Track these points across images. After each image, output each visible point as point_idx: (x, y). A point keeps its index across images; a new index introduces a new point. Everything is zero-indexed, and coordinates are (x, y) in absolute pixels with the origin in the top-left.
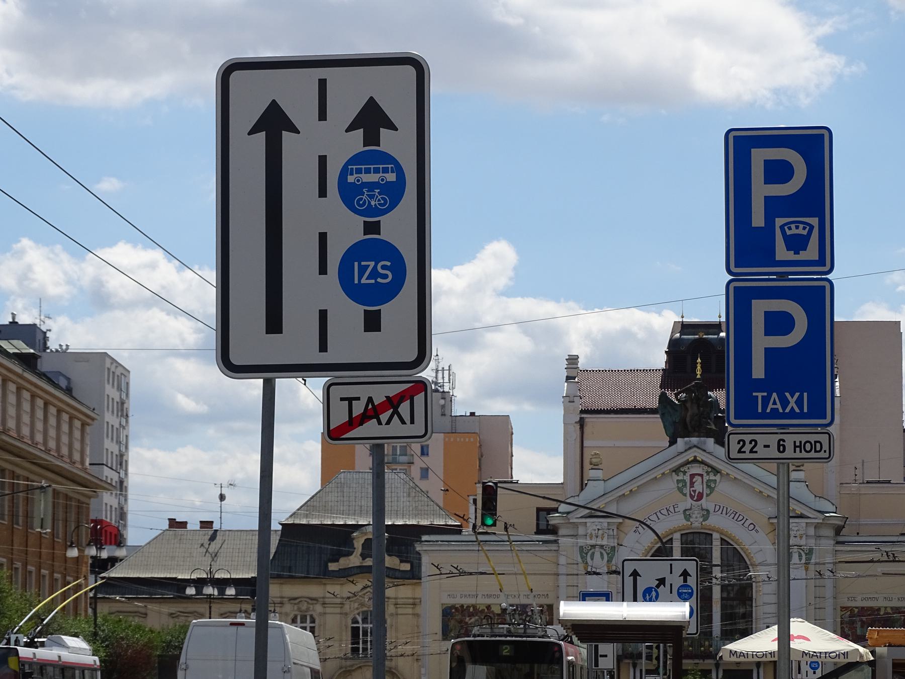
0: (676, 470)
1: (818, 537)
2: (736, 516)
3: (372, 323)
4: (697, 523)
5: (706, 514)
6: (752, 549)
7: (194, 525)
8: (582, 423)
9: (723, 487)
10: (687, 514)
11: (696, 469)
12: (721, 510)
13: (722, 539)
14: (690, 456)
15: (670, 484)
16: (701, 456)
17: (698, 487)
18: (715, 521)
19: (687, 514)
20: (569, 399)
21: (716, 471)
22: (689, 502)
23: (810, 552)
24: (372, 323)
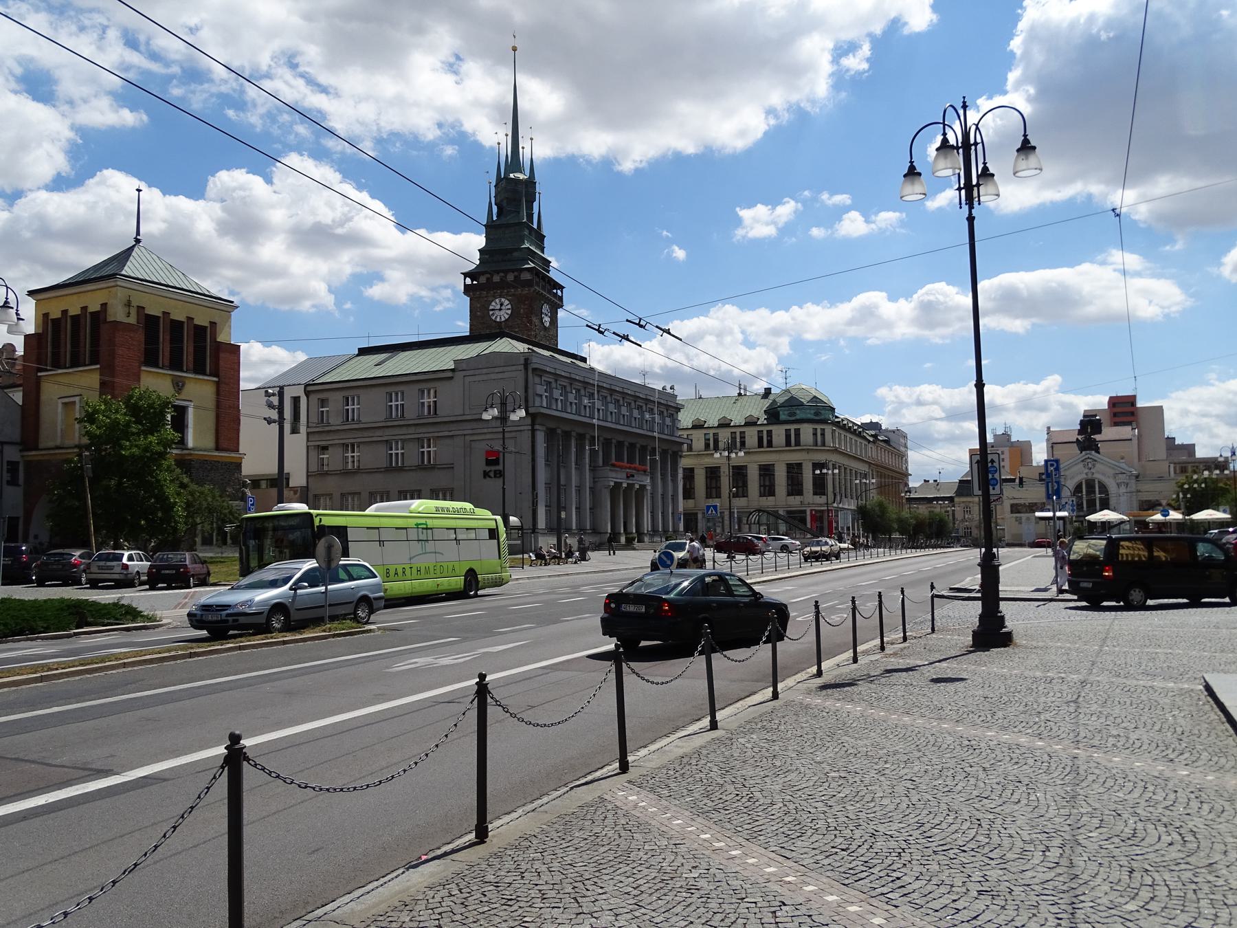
0: (1083, 461)
1: (1130, 479)
2: (1103, 474)
3: (994, 489)
4: (1090, 476)
5: (1093, 473)
6: (1108, 484)
7: (931, 481)
8: (1052, 447)
9: (1098, 466)
10: (1087, 474)
11: (1089, 460)
12: (1098, 472)
13: (1099, 482)
14: (1087, 456)
15: (1081, 465)
16: (1090, 457)
17: (1090, 465)
18: (1096, 476)
19: (1087, 474)
20: (1048, 440)
21: (1095, 461)
22: (1087, 471)
23: (1127, 484)
24: (994, 489)
